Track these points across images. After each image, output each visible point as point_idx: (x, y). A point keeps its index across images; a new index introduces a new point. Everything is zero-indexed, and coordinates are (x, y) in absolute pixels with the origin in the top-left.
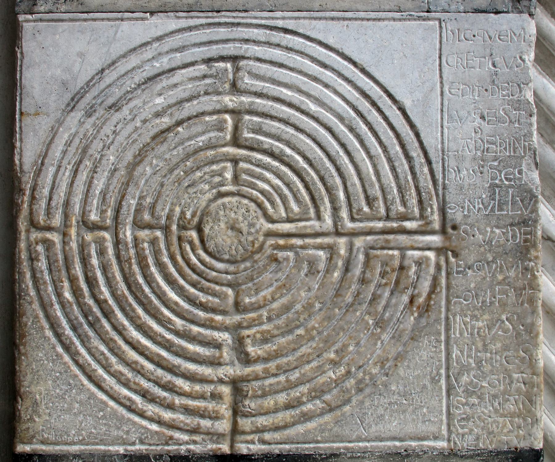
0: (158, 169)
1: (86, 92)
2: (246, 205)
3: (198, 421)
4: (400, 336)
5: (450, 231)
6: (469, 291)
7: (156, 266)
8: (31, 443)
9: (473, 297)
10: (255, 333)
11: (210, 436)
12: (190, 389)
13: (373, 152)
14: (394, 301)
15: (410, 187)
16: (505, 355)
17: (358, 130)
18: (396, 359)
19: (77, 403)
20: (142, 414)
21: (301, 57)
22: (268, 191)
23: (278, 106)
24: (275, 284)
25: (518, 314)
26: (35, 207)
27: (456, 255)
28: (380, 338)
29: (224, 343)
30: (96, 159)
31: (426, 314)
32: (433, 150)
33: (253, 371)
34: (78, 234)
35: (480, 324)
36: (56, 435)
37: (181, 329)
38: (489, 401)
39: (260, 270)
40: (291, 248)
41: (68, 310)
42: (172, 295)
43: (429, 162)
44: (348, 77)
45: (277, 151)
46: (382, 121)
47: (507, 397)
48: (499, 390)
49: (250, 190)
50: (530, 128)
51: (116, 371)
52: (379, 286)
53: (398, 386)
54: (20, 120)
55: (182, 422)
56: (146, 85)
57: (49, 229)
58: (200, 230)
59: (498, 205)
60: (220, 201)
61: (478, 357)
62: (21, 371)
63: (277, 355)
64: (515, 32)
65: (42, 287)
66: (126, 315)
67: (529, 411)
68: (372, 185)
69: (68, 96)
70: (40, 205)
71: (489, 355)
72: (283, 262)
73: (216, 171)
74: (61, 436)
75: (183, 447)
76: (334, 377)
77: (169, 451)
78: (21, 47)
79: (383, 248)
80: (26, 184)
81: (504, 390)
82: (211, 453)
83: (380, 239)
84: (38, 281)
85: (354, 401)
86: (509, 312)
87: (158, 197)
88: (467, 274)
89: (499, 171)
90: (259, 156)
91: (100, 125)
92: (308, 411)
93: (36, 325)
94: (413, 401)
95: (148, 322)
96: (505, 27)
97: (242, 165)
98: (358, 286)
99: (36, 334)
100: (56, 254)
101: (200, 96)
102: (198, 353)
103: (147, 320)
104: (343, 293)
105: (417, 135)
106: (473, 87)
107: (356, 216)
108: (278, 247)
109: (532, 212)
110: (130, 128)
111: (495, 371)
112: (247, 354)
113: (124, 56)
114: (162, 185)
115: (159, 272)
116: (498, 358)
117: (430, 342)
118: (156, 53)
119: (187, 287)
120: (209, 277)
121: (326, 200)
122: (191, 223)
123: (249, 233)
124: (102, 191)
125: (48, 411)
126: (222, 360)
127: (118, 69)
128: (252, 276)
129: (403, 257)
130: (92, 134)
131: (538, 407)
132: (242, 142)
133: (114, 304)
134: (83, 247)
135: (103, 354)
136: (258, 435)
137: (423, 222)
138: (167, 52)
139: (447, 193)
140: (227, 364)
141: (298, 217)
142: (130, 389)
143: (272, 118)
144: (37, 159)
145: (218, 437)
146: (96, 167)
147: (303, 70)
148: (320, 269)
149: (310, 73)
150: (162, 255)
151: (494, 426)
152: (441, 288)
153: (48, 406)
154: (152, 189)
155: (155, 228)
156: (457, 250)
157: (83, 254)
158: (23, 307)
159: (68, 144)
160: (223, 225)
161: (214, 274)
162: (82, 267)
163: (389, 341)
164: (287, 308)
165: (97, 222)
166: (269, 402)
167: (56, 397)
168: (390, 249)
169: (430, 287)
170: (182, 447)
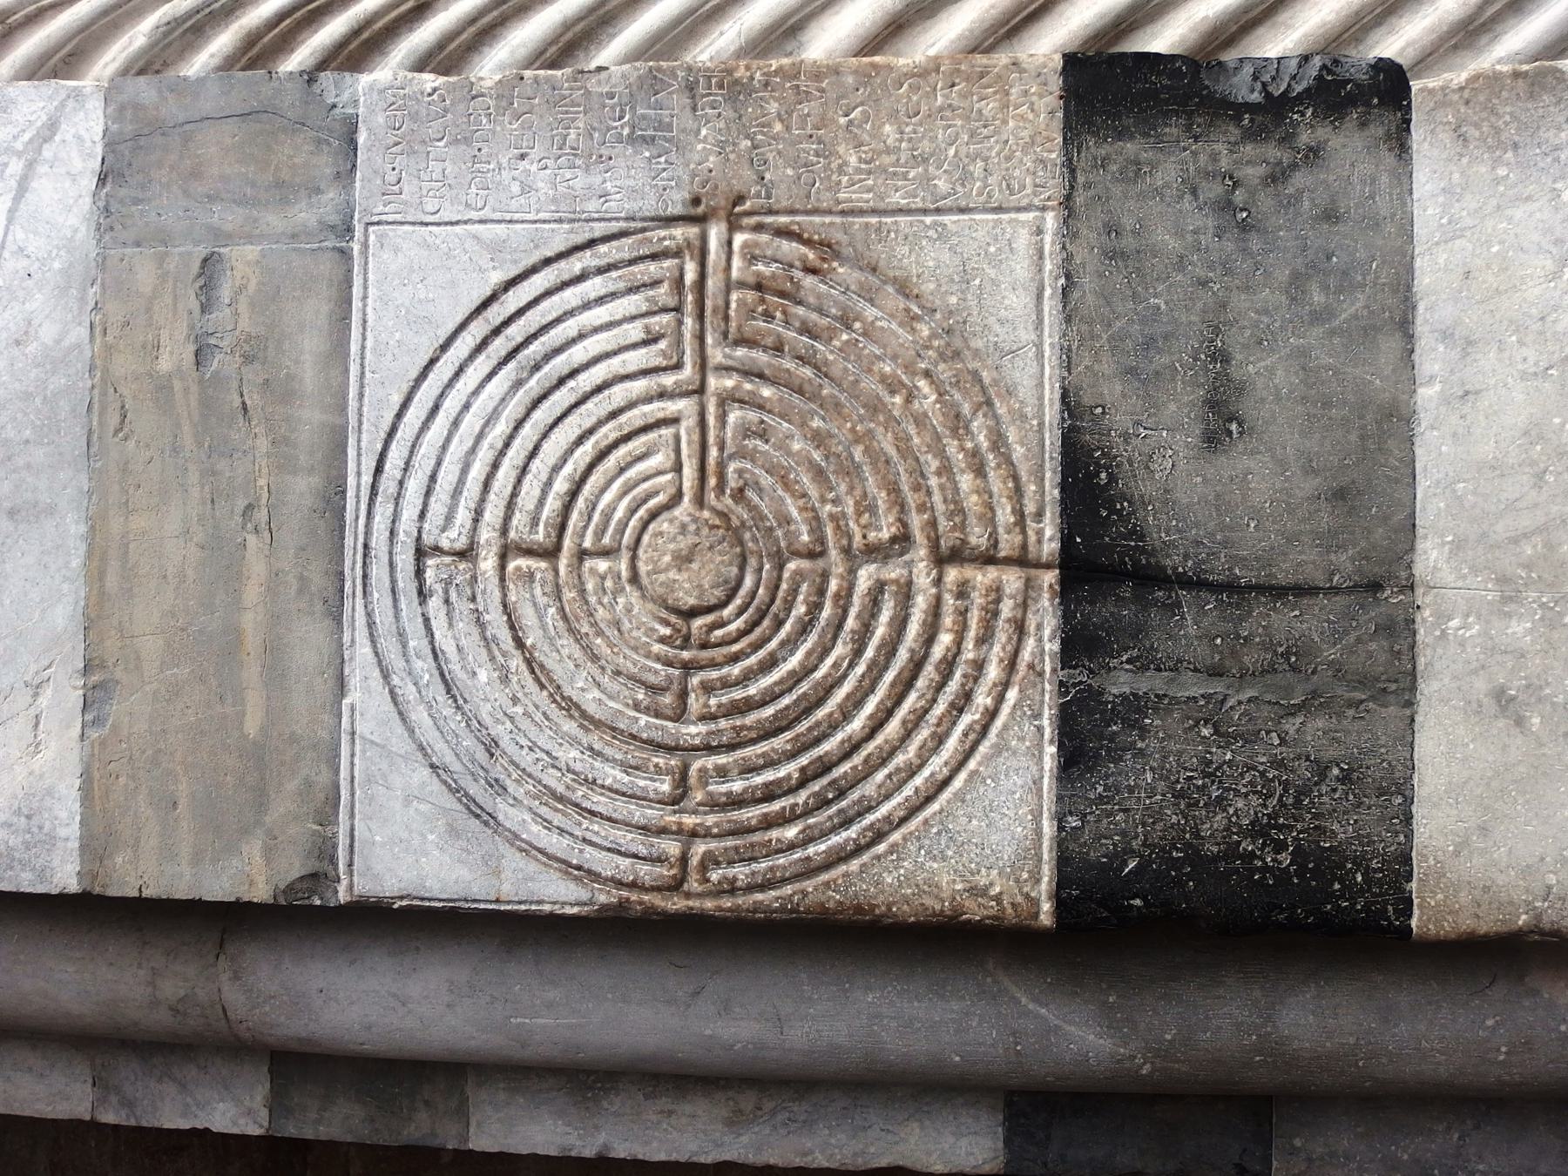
1: (466, 795)
6: (799, 178)
7: (747, 686)
8: (1035, 903)
13: (573, 333)
14: (811, 300)
17: (539, 358)
18: (907, 296)
20: (991, 714)
24: (780, 492)
27: (740, 199)
30: (574, 780)
31: (835, 247)
32: (572, 236)
34: (695, 812)
35: (853, 160)
37: (850, 646)
42: (794, 662)
43: (591, 243)
48: (963, 127)
49: (628, 531)
51: (919, 756)
54: (509, 902)
55: (1004, 649)
57: (684, 859)
58: (692, 613)
60: (645, 581)
62: (915, 915)
63: (894, 490)
64: (389, 102)
65: (778, 874)
67: (999, 76)
71: (904, 145)
75: (1048, 647)
77: (1054, 670)
79: (726, 318)
83: (712, 322)
86: (836, 112)
87: (636, 681)
90: (575, 516)
96: (381, 120)
97: (587, 544)
100: (726, 849)
104: (797, 382)
105: (548, 262)
107: (675, 360)
110: (525, 724)
112: (894, 540)
113: (411, 731)
114: (618, 673)
116: (908, 129)
118: (408, 680)
120: (767, 600)
124: (625, 772)
125: (983, 870)
126: (902, 580)
129: (742, 285)
132: (549, 543)
134: (714, 805)
135: (889, 776)
136: (1028, 522)
138: (407, 661)
140: (911, 572)
141: (673, 456)
142: (947, 734)
143: (514, 494)
146: (586, 780)
149: (446, 433)
150: (729, 675)
152: (792, 223)
155: (686, 687)
157: (726, 804)
159: (547, 824)
161: (761, 591)
164: (819, 474)
165: (674, 780)
166: (972, 502)
167: (961, 856)
170: (1047, 649)
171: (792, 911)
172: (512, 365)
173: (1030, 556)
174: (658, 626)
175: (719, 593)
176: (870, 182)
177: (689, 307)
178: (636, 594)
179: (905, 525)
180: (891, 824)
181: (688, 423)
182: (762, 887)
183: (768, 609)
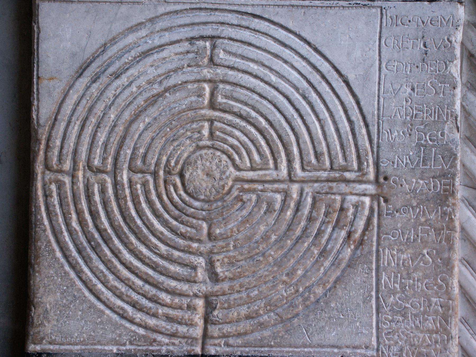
0: (149, 126)
1: (91, 62)
2: (219, 156)
3: (177, 327)
4: (339, 264)
5: (382, 180)
6: (396, 230)
7: (146, 203)
8: (40, 343)
9: (399, 234)
10: (224, 258)
11: (186, 340)
12: (171, 301)
13: (321, 117)
14: (335, 235)
15: (350, 145)
16: (425, 282)
17: (309, 99)
18: (335, 282)
19: (80, 311)
20: (132, 321)
21: (266, 38)
22: (238, 147)
23: (246, 77)
25: (436, 250)
26: (49, 154)
27: (386, 201)
28: (323, 265)
29: (199, 265)
31: (361, 247)
33: (221, 288)
34: (84, 177)
35: (404, 256)
36: (62, 337)
37: (165, 253)
38: (412, 319)
39: (229, 208)
40: (254, 191)
41: (75, 237)
43: (367, 125)
44: (303, 55)
45: (244, 114)
46: (330, 91)
47: (426, 316)
50: (453, 98)
51: (112, 286)
52: (323, 223)
53: (336, 304)
54: (38, 84)
55: (163, 327)
56: (140, 58)
57: (60, 171)
58: (182, 176)
59: (423, 161)
60: (198, 153)
61: (402, 283)
65: (54, 218)
66: (122, 241)
67: (445, 330)
68: (320, 143)
69: (76, 65)
70: (53, 152)
71: (411, 281)
72: (247, 203)
73: (195, 129)
74: (66, 338)
76: (285, 294)
77: (153, 351)
78: (38, 22)
79: (327, 193)
80: (42, 136)
81: (424, 310)
82: (186, 353)
83: (324, 186)
84: (51, 213)
85: (301, 315)
88: (395, 216)
89: (424, 134)
90: (229, 117)
91: (103, 89)
92: (264, 321)
93: (49, 248)
94: (348, 317)
95: (138, 248)
98: (306, 223)
99: (48, 256)
100: (66, 192)
101: (183, 68)
102: (178, 273)
103: (138, 246)
105: (358, 103)
106: (406, 64)
108: (243, 190)
109: (451, 167)
110: (127, 92)
111: (417, 296)
112: (216, 274)
115: (149, 208)
117: (363, 269)
118: (148, 32)
119: (171, 220)
120: (188, 213)
121: (283, 154)
122: (175, 169)
123: (221, 179)
126: (197, 278)
127: (118, 44)
128: (222, 212)
129: (343, 201)
130: (96, 96)
131: (453, 325)
133: (112, 232)
134: (88, 188)
135: (102, 272)
136: (224, 339)
137: (361, 173)
138: (158, 32)
139: (381, 150)
140: (201, 282)
141: (259, 167)
142: (123, 300)
143: (241, 86)
144: (51, 115)
145: (192, 340)
146: (99, 123)
147: (267, 49)
148: (276, 209)
149: (272, 51)
150: (151, 194)
151: (415, 340)
152: (373, 226)
153: (56, 313)
154: (144, 142)
155: (146, 173)
156: (388, 196)
157: (88, 193)
158: (38, 233)
159: (77, 104)
160: (199, 172)
161: (192, 210)
162: (87, 202)
163: (330, 268)
164: (249, 238)
165: (100, 167)
166: (234, 314)
167: (63, 307)
168: (332, 194)
169: (365, 225)
171: (36, 225)
172: (305, 84)
173: (208, 340)
174: (175, 159)
175: (191, 189)
176: (393, 264)
177: (333, 175)
178: (191, 149)
179: (223, 280)
180: (79, 273)
181: (272, 174)
182: (47, 209)
183: (183, 213)
